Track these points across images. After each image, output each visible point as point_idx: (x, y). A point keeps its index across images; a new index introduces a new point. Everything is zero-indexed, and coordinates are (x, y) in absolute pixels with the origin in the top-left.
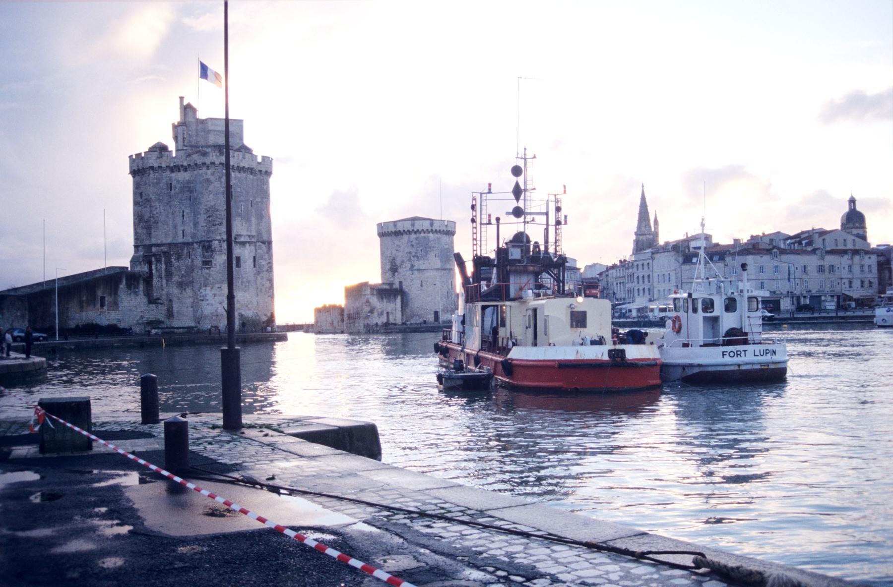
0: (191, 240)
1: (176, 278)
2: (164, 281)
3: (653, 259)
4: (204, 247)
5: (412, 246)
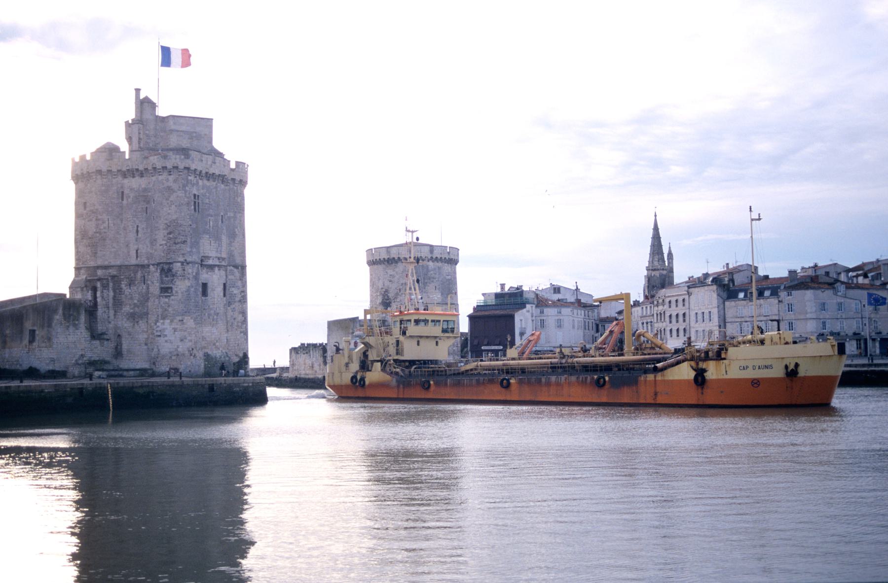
0: (146, 262)
1: (127, 309)
2: (112, 312)
3: (689, 294)
4: (162, 270)
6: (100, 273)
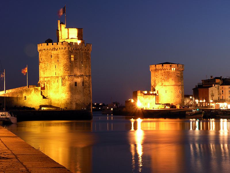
6: (46, 79)
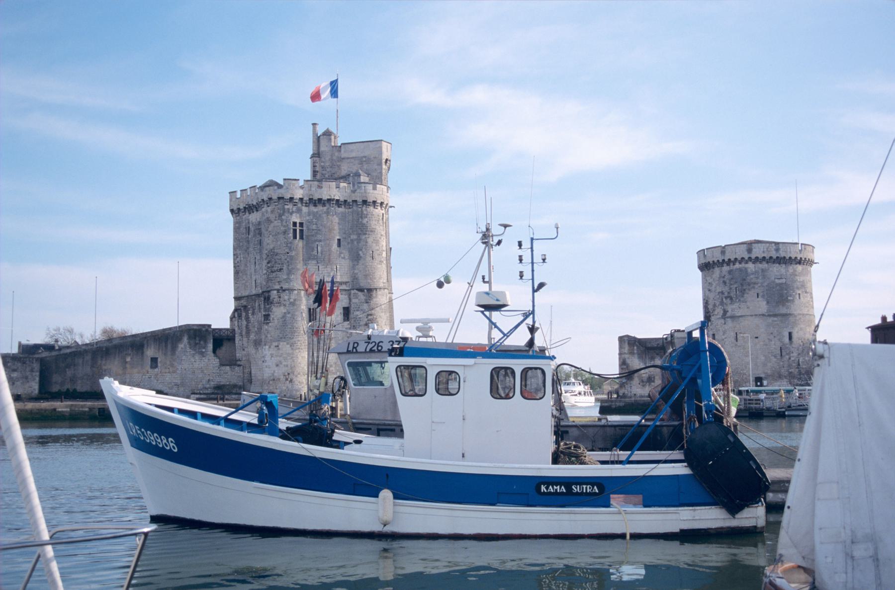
5: (725, 282)
